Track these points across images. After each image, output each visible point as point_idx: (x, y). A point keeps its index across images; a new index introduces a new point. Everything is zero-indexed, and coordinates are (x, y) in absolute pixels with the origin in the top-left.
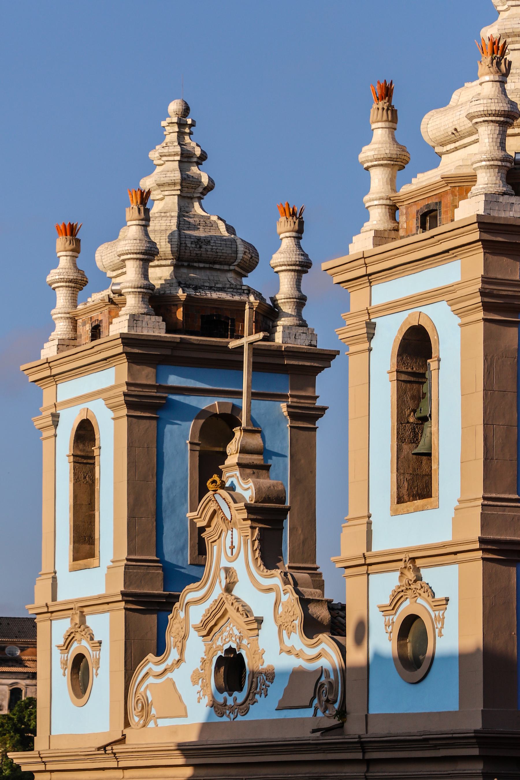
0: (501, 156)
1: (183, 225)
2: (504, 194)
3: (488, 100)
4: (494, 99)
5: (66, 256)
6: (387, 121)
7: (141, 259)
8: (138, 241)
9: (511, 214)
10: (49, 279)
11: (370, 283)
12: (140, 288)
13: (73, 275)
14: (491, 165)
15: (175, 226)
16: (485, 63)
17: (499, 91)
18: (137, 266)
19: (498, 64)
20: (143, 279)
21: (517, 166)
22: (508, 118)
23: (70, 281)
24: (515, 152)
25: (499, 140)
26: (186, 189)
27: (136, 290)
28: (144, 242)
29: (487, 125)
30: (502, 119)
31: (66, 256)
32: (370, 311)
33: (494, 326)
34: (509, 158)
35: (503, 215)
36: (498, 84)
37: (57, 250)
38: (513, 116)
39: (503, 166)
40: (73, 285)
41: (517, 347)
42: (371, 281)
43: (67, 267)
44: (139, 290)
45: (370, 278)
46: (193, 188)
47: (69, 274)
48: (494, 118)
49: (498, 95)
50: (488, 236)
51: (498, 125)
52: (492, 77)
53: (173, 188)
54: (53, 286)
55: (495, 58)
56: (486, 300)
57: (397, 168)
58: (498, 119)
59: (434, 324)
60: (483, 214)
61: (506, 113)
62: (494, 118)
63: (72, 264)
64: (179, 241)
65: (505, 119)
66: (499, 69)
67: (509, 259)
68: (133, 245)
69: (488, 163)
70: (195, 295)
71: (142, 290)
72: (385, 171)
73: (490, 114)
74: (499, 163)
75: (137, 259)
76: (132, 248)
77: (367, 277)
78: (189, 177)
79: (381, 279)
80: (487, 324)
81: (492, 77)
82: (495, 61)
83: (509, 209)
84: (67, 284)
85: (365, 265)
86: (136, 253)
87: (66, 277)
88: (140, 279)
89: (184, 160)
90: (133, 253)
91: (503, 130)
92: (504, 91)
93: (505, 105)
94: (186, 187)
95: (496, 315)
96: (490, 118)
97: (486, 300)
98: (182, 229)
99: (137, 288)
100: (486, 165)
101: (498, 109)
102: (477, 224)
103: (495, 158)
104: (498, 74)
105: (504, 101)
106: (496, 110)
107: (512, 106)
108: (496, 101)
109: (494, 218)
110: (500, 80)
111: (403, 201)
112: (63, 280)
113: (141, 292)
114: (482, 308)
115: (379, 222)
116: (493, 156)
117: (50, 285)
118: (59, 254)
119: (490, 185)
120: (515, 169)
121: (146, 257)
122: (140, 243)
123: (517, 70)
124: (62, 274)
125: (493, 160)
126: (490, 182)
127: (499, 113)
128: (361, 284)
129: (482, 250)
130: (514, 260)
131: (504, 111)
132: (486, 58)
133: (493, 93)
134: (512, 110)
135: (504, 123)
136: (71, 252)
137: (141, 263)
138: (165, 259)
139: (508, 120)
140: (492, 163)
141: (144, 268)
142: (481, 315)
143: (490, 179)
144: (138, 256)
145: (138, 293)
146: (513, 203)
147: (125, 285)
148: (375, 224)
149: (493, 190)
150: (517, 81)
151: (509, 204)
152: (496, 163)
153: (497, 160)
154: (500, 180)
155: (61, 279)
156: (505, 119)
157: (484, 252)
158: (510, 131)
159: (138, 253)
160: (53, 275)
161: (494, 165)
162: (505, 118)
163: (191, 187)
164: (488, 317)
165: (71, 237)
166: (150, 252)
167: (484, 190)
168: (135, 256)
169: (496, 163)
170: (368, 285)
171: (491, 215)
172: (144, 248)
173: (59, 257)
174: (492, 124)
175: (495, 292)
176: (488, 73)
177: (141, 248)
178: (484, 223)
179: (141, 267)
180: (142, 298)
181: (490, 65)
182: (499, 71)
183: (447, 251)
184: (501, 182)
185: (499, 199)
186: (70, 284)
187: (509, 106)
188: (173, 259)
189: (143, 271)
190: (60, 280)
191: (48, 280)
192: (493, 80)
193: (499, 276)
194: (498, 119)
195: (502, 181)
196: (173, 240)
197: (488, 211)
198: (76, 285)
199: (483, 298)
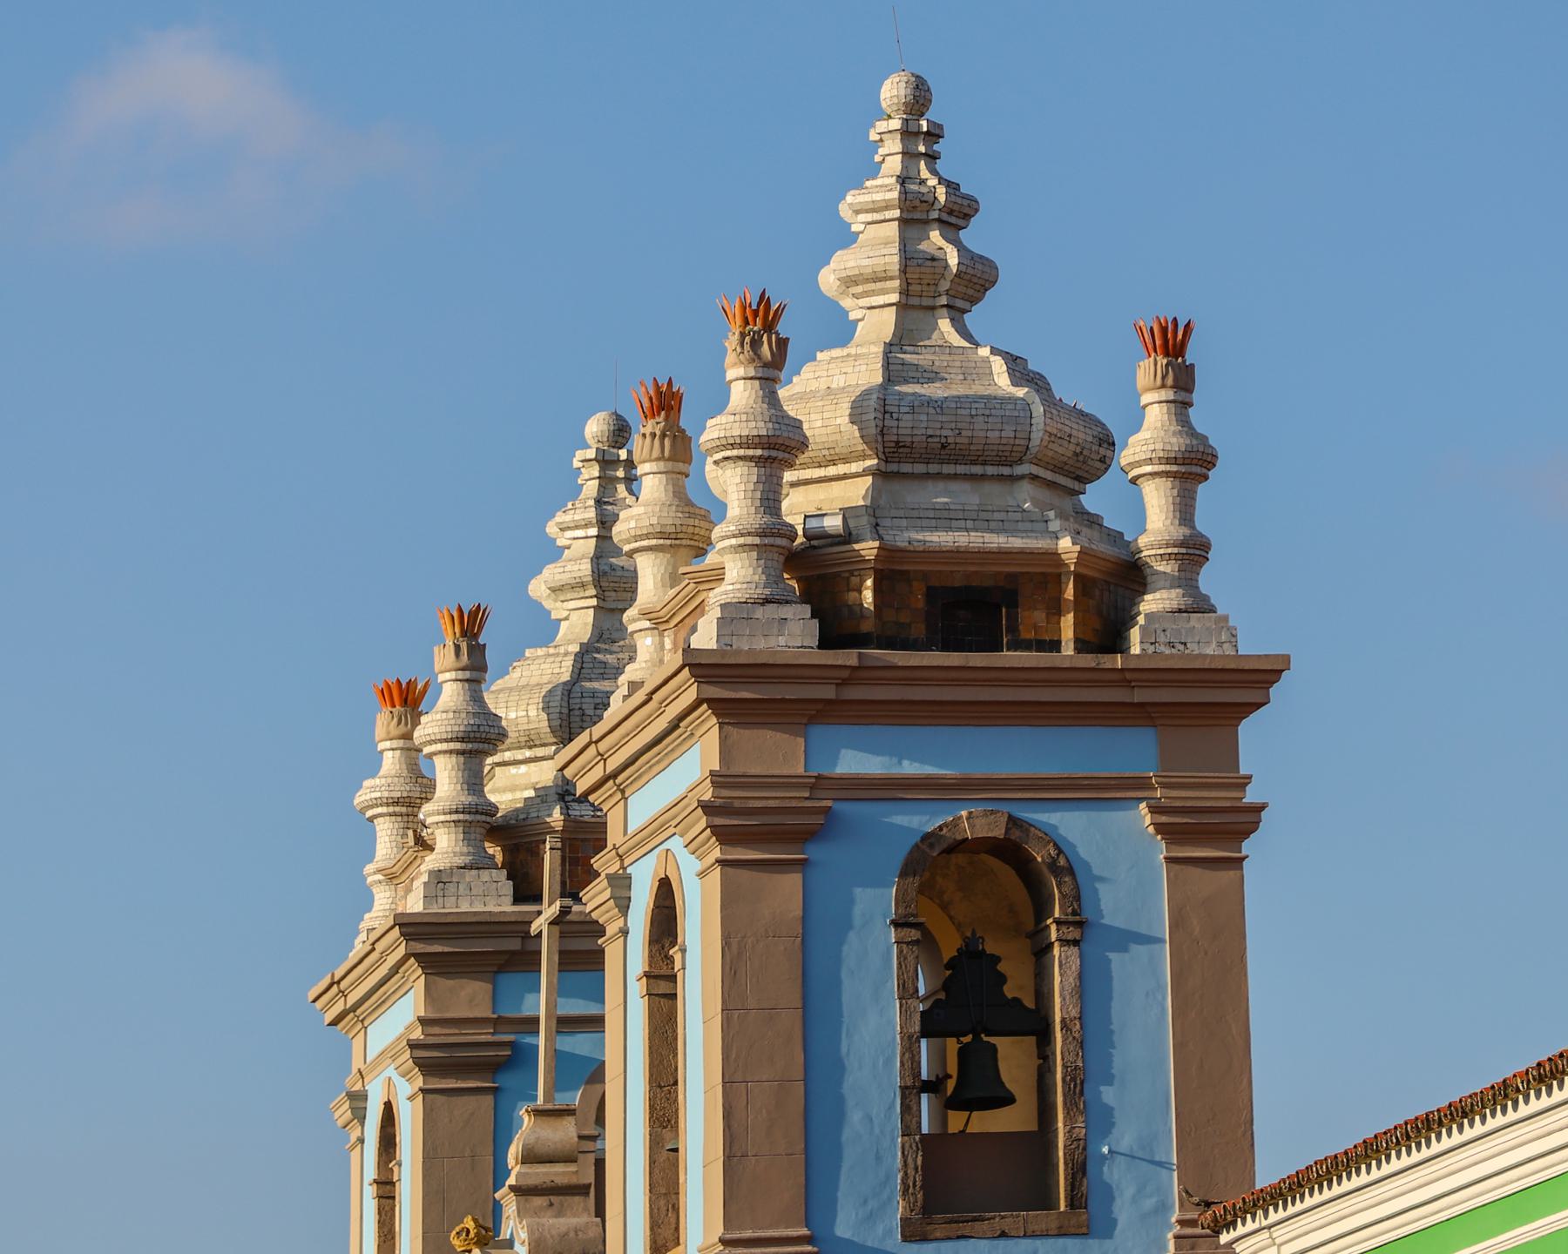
0: (758, 526)
1: (590, 671)
2: (767, 601)
3: (730, 416)
4: (740, 414)
5: (393, 749)
6: (661, 458)
7: (459, 752)
8: (451, 715)
9: (782, 641)
10: (361, 798)
11: (623, 792)
12: (457, 812)
13: (402, 788)
14: (740, 546)
15: (569, 674)
16: (730, 343)
17: (757, 397)
18: (453, 766)
19: (756, 344)
20: (466, 792)
21: (815, 543)
22: (773, 449)
23: (396, 802)
24: (805, 516)
25: (758, 495)
27: (448, 818)
28: (464, 715)
29: (733, 465)
30: (759, 452)
31: (393, 749)
32: (621, 851)
33: (744, 875)
34: (779, 529)
35: (761, 644)
36: (757, 383)
37: (377, 739)
38: (782, 444)
39: (765, 545)
40: (404, 810)
41: (801, 914)
42: (622, 787)
43: (393, 772)
44: (455, 817)
45: (618, 781)
47: (392, 788)
48: (741, 452)
49: (754, 406)
50: (717, 690)
51: (754, 464)
52: (741, 371)
54: (369, 813)
55: (749, 332)
56: (719, 821)
57: (683, 552)
58: (750, 452)
59: (680, 874)
60: (715, 647)
61: (765, 440)
62: (741, 452)
63: (404, 766)
64: (565, 704)
65: (766, 453)
66: (755, 354)
67: (778, 734)
68: (439, 723)
69: (733, 541)
70: (593, 816)
71: (461, 817)
72: (658, 561)
73: (732, 444)
74: (757, 540)
75: (451, 752)
76: (436, 730)
77: (611, 782)
79: (631, 783)
80: (729, 870)
81: (741, 371)
82: (747, 339)
83: (775, 631)
84: (391, 809)
85: (599, 758)
86: (446, 740)
87: (386, 794)
88: (458, 795)
90: (441, 741)
91: (768, 473)
92: (771, 399)
93: (762, 424)
95: (752, 852)
96: (735, 452)
97: (719, 821)
98: (585, 678)
99: (450, 813)
100: (731, 546)
101: (745, 433)
102: (687, 668)
103: (746, 531)
104: (754, 365)
105: (759, 418)
106: (741, 436)
107: (777, 426)
108: (744, 417)
109: (739, 652)
110: (759, 375)
111: (667, 621)
112: (379, 801)
113: (459, 821)
114: (714, 838)
115: (644, 665)
116: (741, 527)
117: (362, 811)
118: (381, 746)
119: (739, 586)
120: (814, 547)
121: (470, 746)
122: (454, 717)
123: (859, 348)
124: (378, 789)
125: (742, 535)
126: (741, 580)
127: (750, 442)
128: (611, 795)
129: (714, 720)
130: (791, 735)
131: (759, 436)
132: (734, 333)
133: (744, 402)
134: (778, 433)
135: (766, 459)
136: (402, 741)
137: (461, 759)
138: (542, 745)
139: (774, 453)
140: (741, 540)
141: (470, 770)
142: (717, 853)
143: (743, 572)
144: (452, 746)
145: (452, 824)
146: (786, 619)
147: (431, 809)
148: (636, 670)
149: (742, 596)
150: (850, 370)
151: (776, 624)
152: (749, 540)
153: (749, 534)
154: (763, 573)
155: (376, 799)
156: (766, 453)
157: (719, 723)
158: (789, 476)
159: (451, 740)
160: (370, 791)
161: (745, 545)
162: (765, 451)
164: (729, 857)
165: (402, 709)
166: (478, 735)
167: (725, 596)
168: (444, 746)
169: (749, 540)
170: (619, 796)
171: (734, 647)
172: (462, 728)
173: (382, 752)
174: (741, 463)
175: (737, 804)
176: (736, 364)
177: (456, 728)
178: (700, 665)
179: (462, 767)
180: (464, 833)
181: (739, 350)
182: (756, 358)
183: (674, 726)
184: (764, 577)
185: (754, 612)
186: (397, 809)
187: (770, 425)
188: (556, 743)
189: (466, 775)
190: (375, 802)
191: (356, 802)
192: (744, 376)
193: (753, 771)
194: (750, 452)
195: (768, 576)
196: (550, 704)
197: (727, 640)
198: (411, 809)
199: (710, 818)
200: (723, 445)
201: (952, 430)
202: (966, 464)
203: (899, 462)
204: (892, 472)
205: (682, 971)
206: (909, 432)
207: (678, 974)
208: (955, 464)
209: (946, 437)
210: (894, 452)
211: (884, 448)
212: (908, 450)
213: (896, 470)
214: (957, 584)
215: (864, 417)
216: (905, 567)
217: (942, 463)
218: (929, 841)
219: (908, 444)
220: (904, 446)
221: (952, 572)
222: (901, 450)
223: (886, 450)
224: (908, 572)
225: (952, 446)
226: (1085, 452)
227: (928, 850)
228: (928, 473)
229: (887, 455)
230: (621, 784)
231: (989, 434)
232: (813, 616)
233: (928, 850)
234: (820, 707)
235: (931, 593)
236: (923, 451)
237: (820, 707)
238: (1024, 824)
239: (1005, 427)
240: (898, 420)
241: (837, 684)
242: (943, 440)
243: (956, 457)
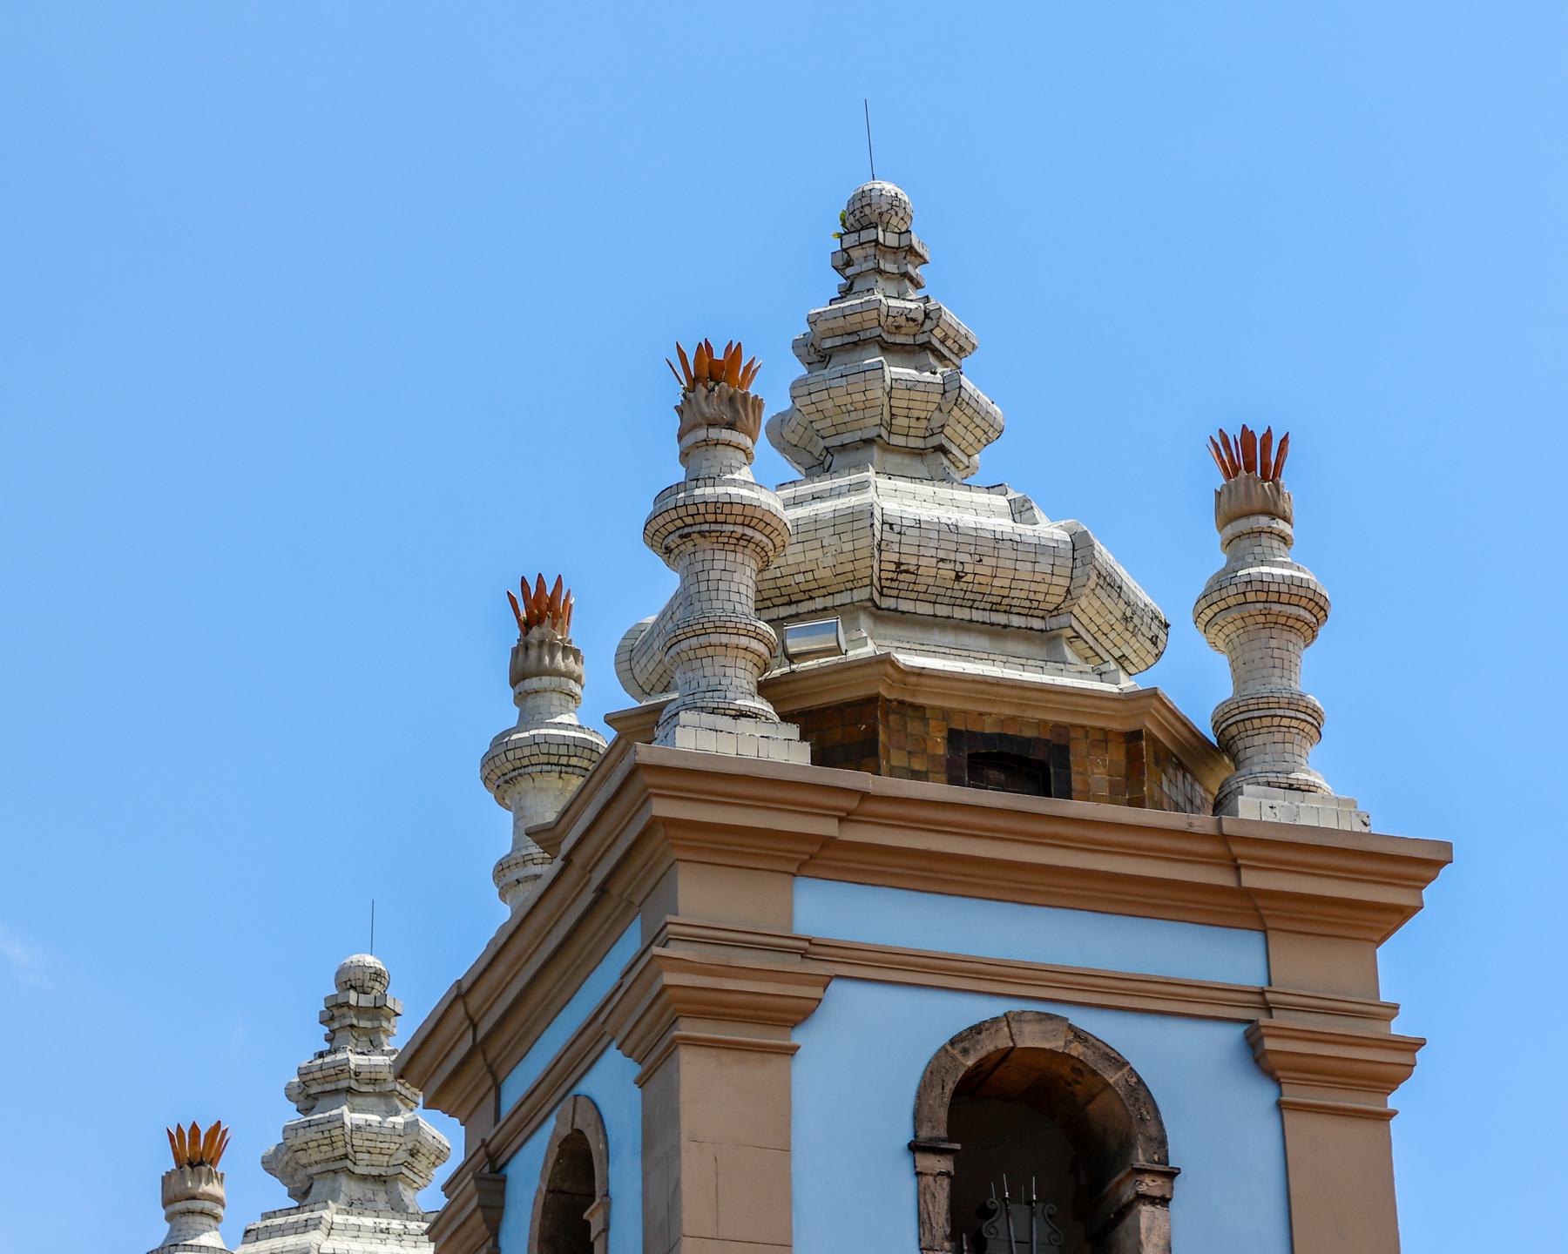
22: (748, 526)
26: (367, 1156)
46: (384, 1151)
53: (329, 1155)
78: (370, 1125)
89: (362, 1090)
94: (364, 1149)
135: (738, 539)
163: (378, 1151)
200: (681, 518)
201: (970, 554)
202: (984, 609)
203: (897, 597)
204: (888, 609)
205: (603, 1235)
206: (914, 550)
207: (596, 1243)
208: (971, 607)
209: (962, 563)
210: (892, 580)
211: (881, 570)
212: (911, 578)
213: (893, 607)
214: (987, 731)
215: (856, 525)
216: (920, 700)
217: (954, 605)
218: (962, 1044)
219: (912, 569)
220: (907, 572)
221: (981, 714)
222: (902, 577)
223: (884, 575)
224: (922, 708)
225: (969, 578)
226: (1136, 620)
227: (959, 1057)
228: (935, 616)
229: (884, 583)
230: (494, 1061)
231: (1019, 565)
232: (803, 738)
233: (959, 1057)
234: (815, 849)
235: (954, 737)
236: (931, 581)
237: (815, 849)
238: (1090, 1038)
239: (1040, 558)
240: (899, 533)
241: (841, 820)
242: (959, 568)
243: (972, 596)
